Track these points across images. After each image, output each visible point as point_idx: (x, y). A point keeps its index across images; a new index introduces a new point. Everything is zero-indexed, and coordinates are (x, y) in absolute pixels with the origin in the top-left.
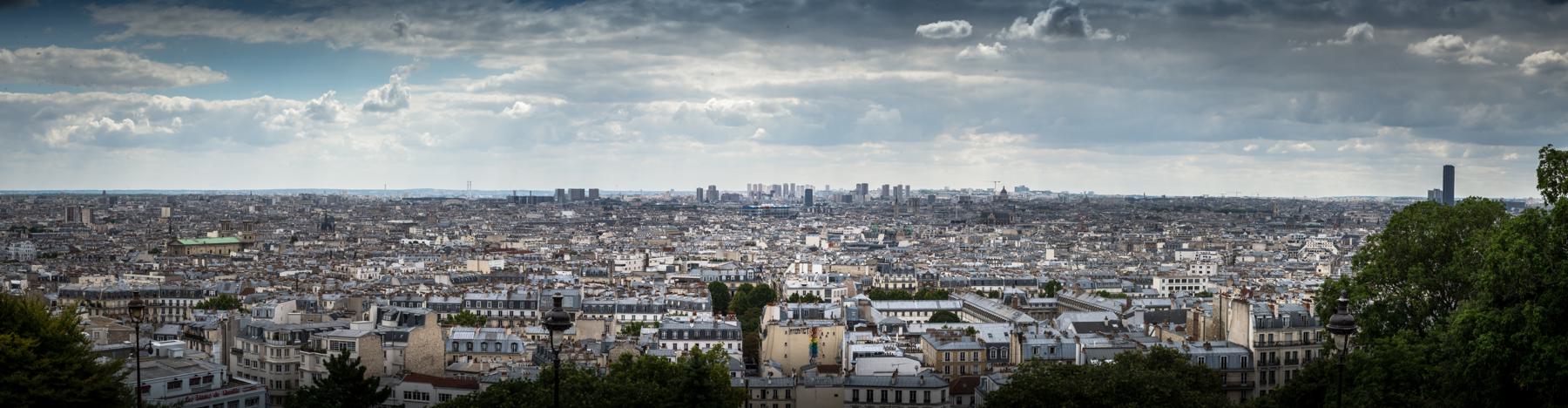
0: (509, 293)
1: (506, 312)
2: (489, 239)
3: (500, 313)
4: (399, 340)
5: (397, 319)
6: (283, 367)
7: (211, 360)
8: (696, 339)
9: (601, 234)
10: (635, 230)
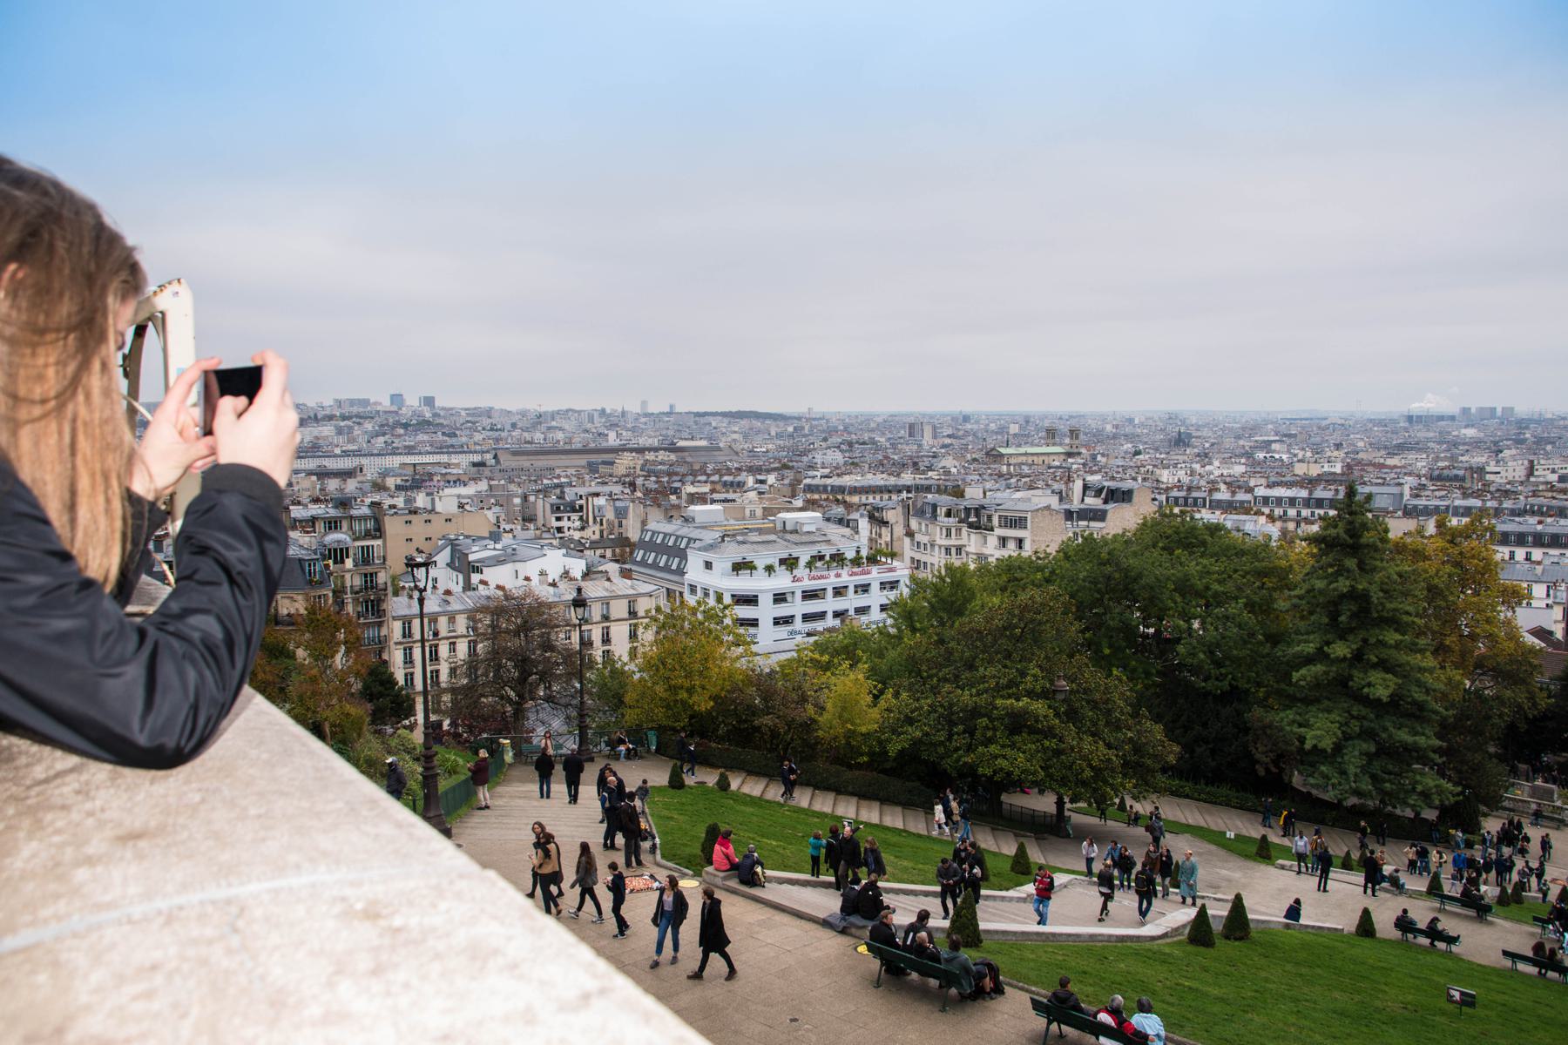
0: (1311, 493)
1: (1305, 513)
2: (1361, 456)
3: (1299, 514)
4: (1094, 519)
5: (1103, 496)
6: (953, 551)
7: (856, 536)
8: (1542, 545)
9: (1501, 452)
10: (1549, 447)
